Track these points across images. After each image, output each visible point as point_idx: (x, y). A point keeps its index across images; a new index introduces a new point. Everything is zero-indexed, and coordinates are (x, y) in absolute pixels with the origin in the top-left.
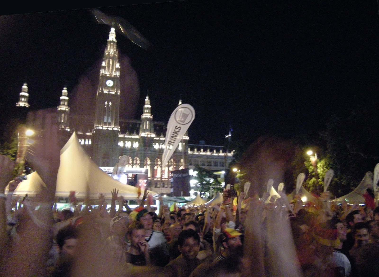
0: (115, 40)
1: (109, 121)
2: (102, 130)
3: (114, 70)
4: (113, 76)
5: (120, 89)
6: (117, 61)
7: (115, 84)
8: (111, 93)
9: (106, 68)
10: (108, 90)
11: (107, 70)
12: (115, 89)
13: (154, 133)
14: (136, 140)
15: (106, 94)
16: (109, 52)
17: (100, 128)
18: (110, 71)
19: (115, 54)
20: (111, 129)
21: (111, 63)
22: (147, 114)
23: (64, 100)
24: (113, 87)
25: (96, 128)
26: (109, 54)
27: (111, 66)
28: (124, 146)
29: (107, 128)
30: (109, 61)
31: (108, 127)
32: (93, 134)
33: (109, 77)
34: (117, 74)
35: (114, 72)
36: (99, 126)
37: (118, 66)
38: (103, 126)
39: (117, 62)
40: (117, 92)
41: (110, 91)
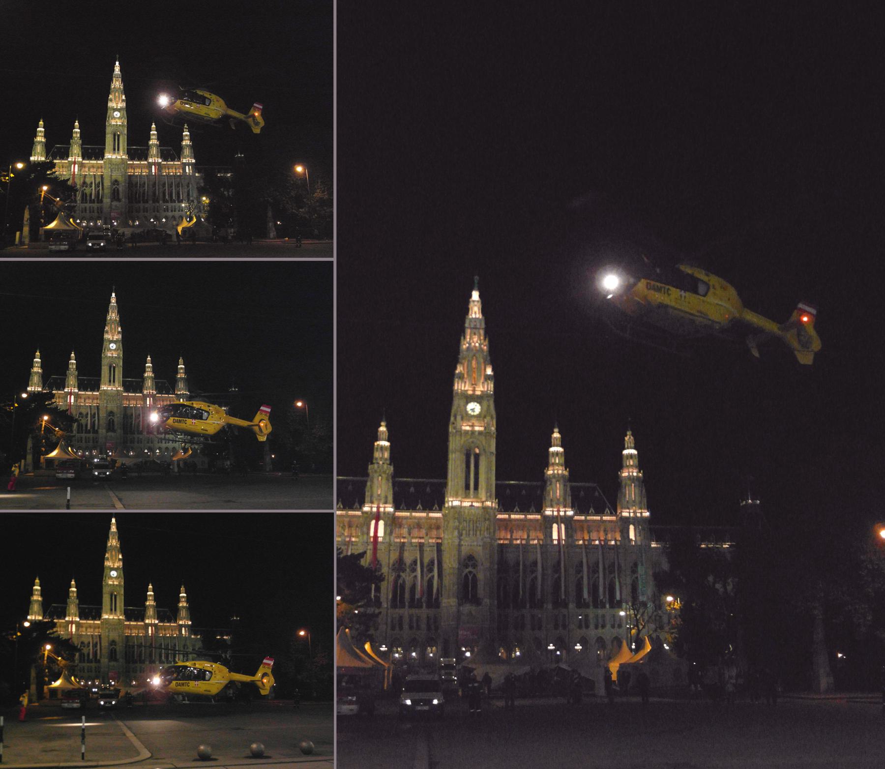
3: (483, 377)
10: (470, 424)
17: (456, 503)
33: (471, 395)
34: (488, 388)
36: (455, 499)
38: (463, 500)
41: (473, 426)
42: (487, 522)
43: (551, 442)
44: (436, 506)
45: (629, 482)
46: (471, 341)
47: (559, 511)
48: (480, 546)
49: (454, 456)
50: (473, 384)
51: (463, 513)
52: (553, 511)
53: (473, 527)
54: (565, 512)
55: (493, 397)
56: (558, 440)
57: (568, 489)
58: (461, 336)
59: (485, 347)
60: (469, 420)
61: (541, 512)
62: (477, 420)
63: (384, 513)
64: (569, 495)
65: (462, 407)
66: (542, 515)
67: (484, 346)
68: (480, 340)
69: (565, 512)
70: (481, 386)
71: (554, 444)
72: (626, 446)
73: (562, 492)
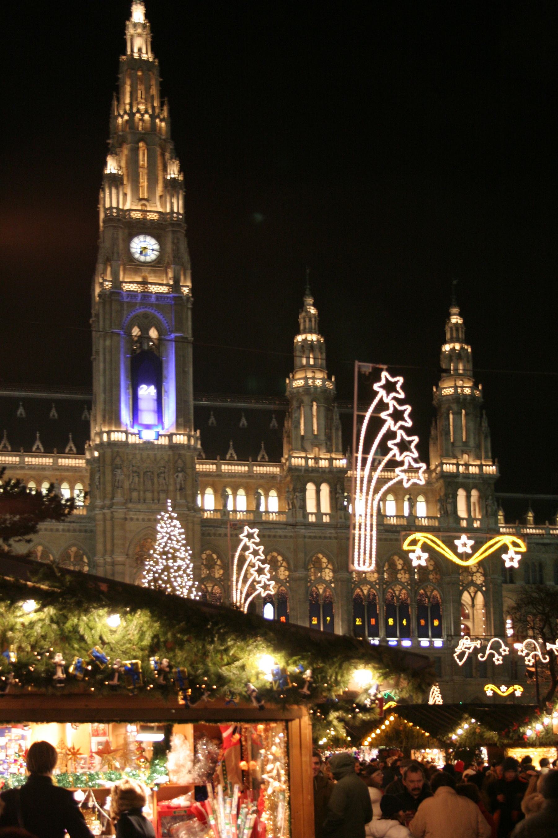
0: (148, 56)
2: (125, 444)
5: (189, 273)
6: (170, 146)
7: (169, 247)
9: (122, 184)
10: (140, 279)
12: (170, 275)
16: (132, 115)
19: (157, 121)
21: (143, 160)
25: (101, 439)
26: (131, 123)
27: (146, 171)
28: (224, 512)
30: (135, 151)
32: (88, 462)
35: (161, 197)
39: (168, 156)
40: (176, 287)
41: (144, 283)
43: (298, 324)
44: (71, 444)
46: (135, 110)
47: (317, 459)
49: (108, 343)
51: (130, 457)
52: (306, 459)
53: (153, 484)
54: (331, 460)
55: (184, 225)
56: (313, 320)
58: (111, 100)
59: (163, 124)
61: (280, 461)
62: (154, 272)
65: (121, 245)
66: (282, 466)
67: (161, 121)
68: (153, 108)
70: (158, 204)
71: (305, 328)
73: (323, 422)
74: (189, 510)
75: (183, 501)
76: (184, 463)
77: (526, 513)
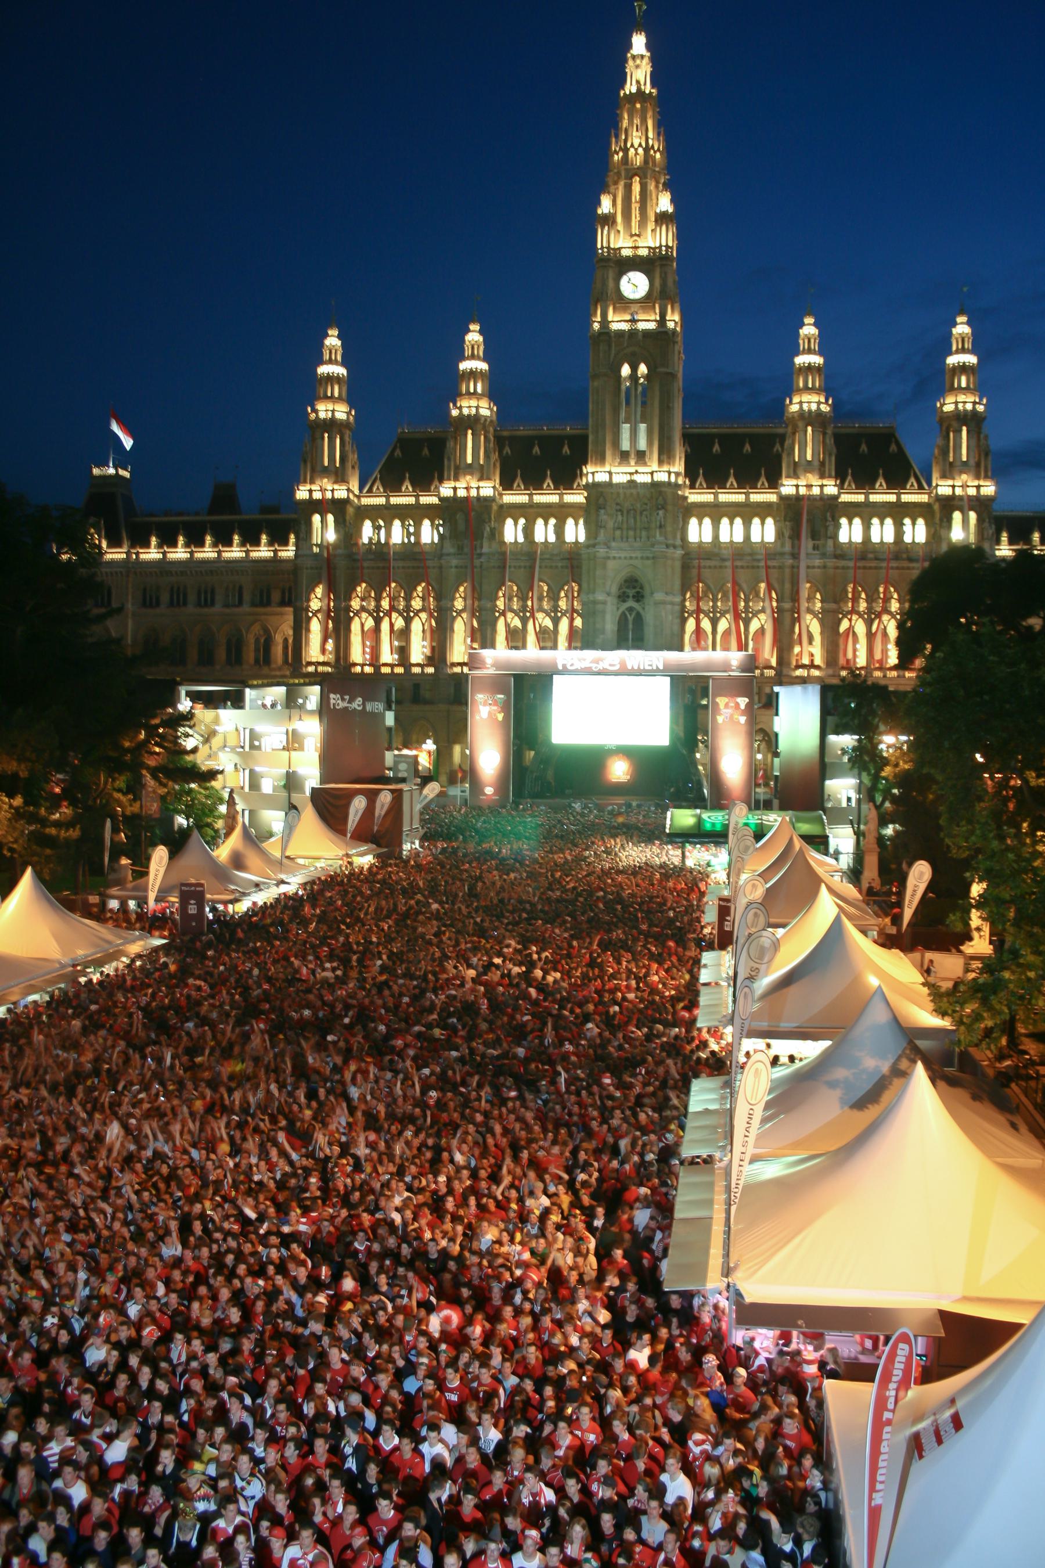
1: (642, 444)
2: (609, 484)
4: (643, 252)
5: (677, 306)
8: (641, 326)
9: (614, 222)
10: (628, 317)
11: (620, 227)
13: (840, 476)
14: (763, 511)
15: (620, 333)
16: (626, 150)
17: (602, 477)
18: (635, 230)
20: (646, 479)
22: (806, 398)
23: (473, 374)
24: (647, 302)
29: (631, 474)
30: (628, 188)
31: (632, 470)
36: (599, 469)
37: (664, 203)
38: (614, 470)
40: (662, 321)
41: (633, 321)
42: (661, 512)
45: (955, 424)
47: (809, 486)
48: (648, 558)
50: (632, 236)
57: (830, 441)
59: (658, 156)
60: (625, 309)
63: (479, 498)
64: (830, 455)
65: (611, 284)
69: (822, 486)
72: (954, 348)
74: (667, 546)
75: (662, 539)
76: (665, 500)
77: (1031, 532)
